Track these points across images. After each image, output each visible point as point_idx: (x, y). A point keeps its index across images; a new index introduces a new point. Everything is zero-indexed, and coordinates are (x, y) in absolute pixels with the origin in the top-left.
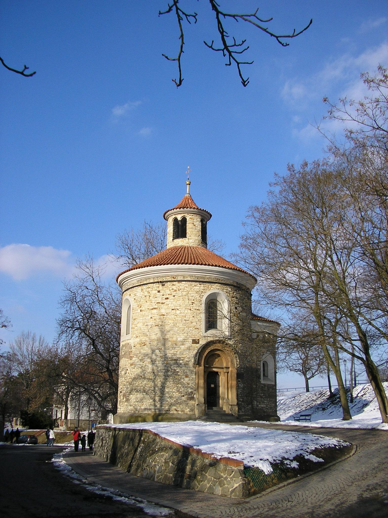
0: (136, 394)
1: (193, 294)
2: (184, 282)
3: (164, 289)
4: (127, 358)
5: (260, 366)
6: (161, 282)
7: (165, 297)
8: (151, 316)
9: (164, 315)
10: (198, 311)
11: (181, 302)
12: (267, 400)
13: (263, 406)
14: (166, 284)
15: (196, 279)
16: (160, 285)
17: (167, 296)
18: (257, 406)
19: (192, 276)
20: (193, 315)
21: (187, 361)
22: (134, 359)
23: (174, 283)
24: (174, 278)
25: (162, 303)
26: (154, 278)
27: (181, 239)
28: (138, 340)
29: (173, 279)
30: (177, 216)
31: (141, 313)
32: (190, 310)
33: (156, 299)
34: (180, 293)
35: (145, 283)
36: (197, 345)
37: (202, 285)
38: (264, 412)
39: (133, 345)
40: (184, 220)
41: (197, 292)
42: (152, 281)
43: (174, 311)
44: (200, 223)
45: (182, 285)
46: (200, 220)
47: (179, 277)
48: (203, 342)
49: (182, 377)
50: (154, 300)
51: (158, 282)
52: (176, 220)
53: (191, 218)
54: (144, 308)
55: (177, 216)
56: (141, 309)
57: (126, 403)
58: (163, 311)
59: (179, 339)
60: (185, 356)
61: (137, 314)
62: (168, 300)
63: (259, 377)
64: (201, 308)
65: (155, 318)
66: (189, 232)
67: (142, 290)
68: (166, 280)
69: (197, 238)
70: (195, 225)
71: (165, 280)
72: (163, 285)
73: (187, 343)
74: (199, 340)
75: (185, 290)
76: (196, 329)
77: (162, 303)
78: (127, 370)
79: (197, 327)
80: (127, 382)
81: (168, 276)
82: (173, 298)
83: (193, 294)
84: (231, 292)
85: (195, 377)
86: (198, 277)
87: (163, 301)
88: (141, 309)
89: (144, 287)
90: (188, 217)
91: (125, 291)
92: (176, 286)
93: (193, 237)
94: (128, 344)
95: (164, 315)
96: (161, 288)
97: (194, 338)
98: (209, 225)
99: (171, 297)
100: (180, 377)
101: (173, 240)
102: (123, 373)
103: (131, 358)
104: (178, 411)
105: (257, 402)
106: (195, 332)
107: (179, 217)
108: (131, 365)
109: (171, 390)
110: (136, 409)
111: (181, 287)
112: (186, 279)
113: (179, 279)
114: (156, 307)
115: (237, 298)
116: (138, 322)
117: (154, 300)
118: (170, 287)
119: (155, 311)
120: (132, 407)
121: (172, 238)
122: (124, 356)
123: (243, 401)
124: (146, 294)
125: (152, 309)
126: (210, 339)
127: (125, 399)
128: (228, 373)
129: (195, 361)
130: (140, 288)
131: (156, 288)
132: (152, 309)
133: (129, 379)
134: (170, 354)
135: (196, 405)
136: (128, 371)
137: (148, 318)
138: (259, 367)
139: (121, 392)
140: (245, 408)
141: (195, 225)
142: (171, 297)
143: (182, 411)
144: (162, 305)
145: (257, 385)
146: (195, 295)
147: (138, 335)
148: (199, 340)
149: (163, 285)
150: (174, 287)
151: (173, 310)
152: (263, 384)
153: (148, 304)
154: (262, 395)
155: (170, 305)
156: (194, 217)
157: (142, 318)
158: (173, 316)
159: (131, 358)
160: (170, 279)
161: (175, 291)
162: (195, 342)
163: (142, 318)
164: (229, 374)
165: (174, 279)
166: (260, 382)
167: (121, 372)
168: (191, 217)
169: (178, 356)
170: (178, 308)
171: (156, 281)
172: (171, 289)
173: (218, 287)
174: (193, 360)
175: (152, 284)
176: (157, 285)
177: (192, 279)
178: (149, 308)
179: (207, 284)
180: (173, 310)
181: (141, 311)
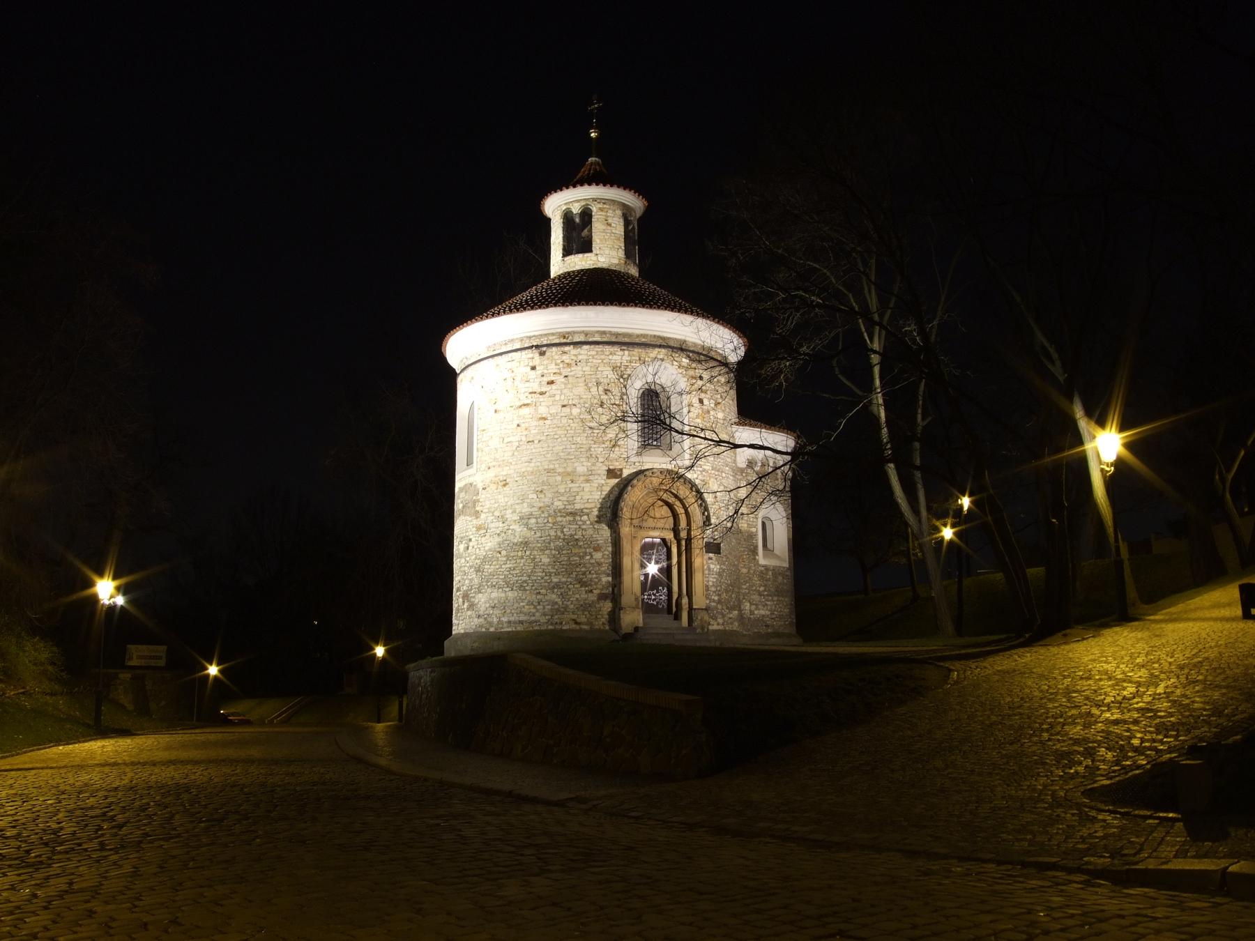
0: (489, 590)
6: (537, 347)
7: (546, 379)
9: (545, 419)
11: (581, 390)
13: (763, 612)
16: (537, 355)
17: (552, 378)
18: (752, 612)
22: (483, 516)
23: (566, 348)
25: (542, 393)
27: (580, 256)
34: (577, 370)
38: (767, 626)
39: (480, 486)
40: (586, 215)
41: (614, 368)
43: (567, 410)
44: (622, 221)
53: (601, 209)
56: (496, 407)
57: (469, 613)
58: (543, 410)
62: (553, 386)
63: (754, 551)
69: (614, 253)
72: (542, 354)
77: (542, 393)
80: (471, 567)
86: (617, 335)
87: (543, 390)
96: (537, 359)
99: (560, 379)
102: (462, 547)
103: (477, 514)
105: (751, 604)
107: (576, 209)
108: (479, 528)
110: (491, 624)
113: (577, 339)
119: (526, 411)
120: (481, 620)
122: (462, 512)
123: (719, 602)
138: (754, 530)
139: (458, 590)
140: (724, 616)
141: (609, 225)
144: (541, 398)
145: (749, 569)
150: (565, 357)
155: (557, 398)
159: (477, 514)
161: (569, 365)
167: (458, 547)
169: (578, 506)
175: (519, 353)
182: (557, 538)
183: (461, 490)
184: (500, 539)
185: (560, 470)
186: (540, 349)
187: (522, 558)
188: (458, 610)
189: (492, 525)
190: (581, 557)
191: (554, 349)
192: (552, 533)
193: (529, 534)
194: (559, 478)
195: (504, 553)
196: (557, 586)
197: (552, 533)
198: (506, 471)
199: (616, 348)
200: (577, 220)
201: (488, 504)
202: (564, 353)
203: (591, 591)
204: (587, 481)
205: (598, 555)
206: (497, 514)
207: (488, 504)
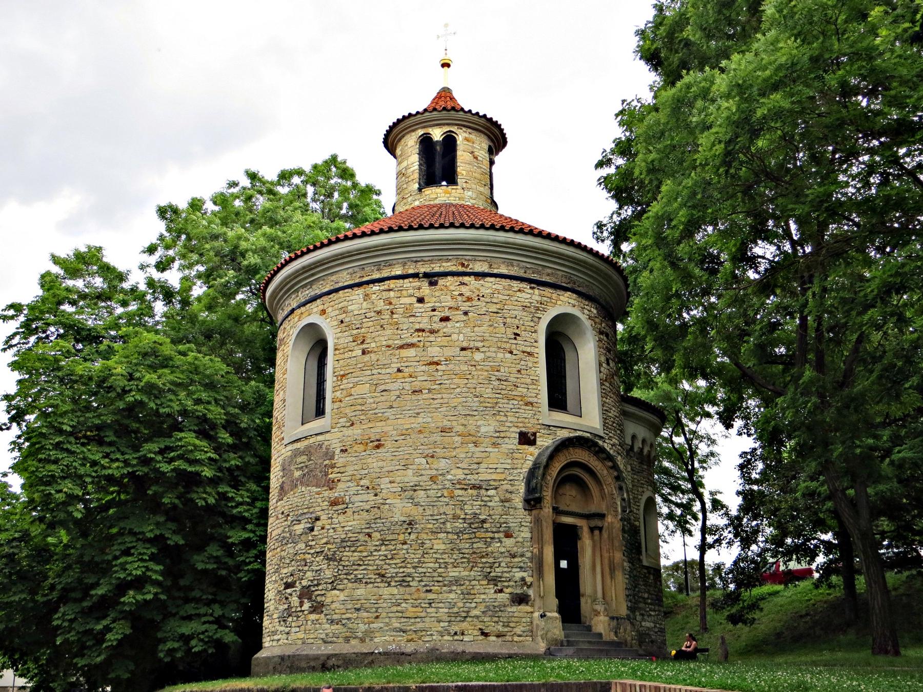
0: (350, 585)
1: (516, 312)
2: (492, 279)
3: (437, 294)
4: (317, 486)
5: (638, 519)
6: (426, 275)
8: (399, 365)
10: (531, 358)
12: (655, 611)
14: (441, 282)
15: (521, 274)
16: (425, 284)
17: (447, 313)
19: (513, 266)
20: (519, 367)
21: (507, 491)
22: (341, 486)
23: (466, 279)
24: (463, 265)
25: (432, 332)
26: (404, 264)
28: (356, 431)
29: (461, 269)
30: (430, 130)
31: (366, 358)
32: (511, 352)
33: (412, 319)
34: (482, 306)
35: (376, 276)
36: (531, 449)
37: (536, 291)
38: (652, 642)
40: (450, 142)
42: (399, 273)
43: (468, 353)
44: (487, 155)
45: (487, 285)
46: (486, 147)
47: (479, 263)
48: (545, 442)
49: (496, 535)
50: (405, 323)
51: (415, 276)
52: (426, 142)
53: (466, 139)
54: (373, 345)
55: (430, 130)
56: (364, 346)
57: (313, 617)
58: (434, 352)
59: (483, 429)
60: (502, 477)
61: (353, 361)
62: (449, 324)
64: (536, 350)
65: (411, 369)
66: (464, 173)
67: (367, 296)
68: (442, 270)
69: (482, 189)
70: (476, 158)
71: (437, 270)
72: (433, 284)
73: (506, 440)
74: (534, 434)
75: (495, 300)
76: (526, 404)
77: (432, 332)
78: (317, 519)
79: (531, 400)
81: (448, 260)
82: (465, 318)
83: (516, 312)
84: (597, 320)
85: (528, 535)
87: (435, 326)
88: (364, 346)
89: (376, 288)
90: (461, 136)
91: (304, 304)
92: (471, 287)
93: (474, 186)
94: (320, 446)
95: (438, 364)
96: (425, 289)
97: (523, 429)
98: (495, 169)
99: (458, 316)
100: (491, 535)
101: (420, 190)
103: (331, 485)
104: (485, 634)
106: (527, 412)
107: (437, 134)
108: (334, 503)
109: (467, 573)
111: (484, 291)
112: (495, 271)
113: (479, 267)
114: (415, 340)
115: (607, 335)
116: (356, 385)
117: (405, 323)
118: (452, 288)
119: (411, 352)
121: (417, 186)
124: (380, 306)
125: (402, 347)
126: (564, 434)
127: (307, 605)
128: (600, 529)
129: (530, 490)
130: (360, 291)
131: (411, 291)
132: (402, 347)
133: (326, 543)
134: (460, 471)
135: (536, 614)
136: (319, 523)
137: (388, 371)
138: (637, 523)
139: (288, 586)
141: (476, 158)
142: (458, 316)
143: (498, 636)
146: (519, 313)
147: (353, 419)
148: (534, 434)
149: (433, 284)
150: (464, 289)
151: (463, 349)
152: (647, 568)
153: (388, 332)
154: (646, 595)
155: (454, 337)
156: (474, 136)
157: (369, 372)
158: (464, 368)
159: (331, 485)
160: (454, 269)
161: (469, 299)
162: (526, 439)
163: (369, 372)
164: (605, 535)
165: (464, 269)
166: (640, 561)
168: (467, 135)
169: (483, 477)
170: (480, 344)
171: (411, 271)
172: (457, 293)
173: (572, 302)
174: (522, 489)
175: (401, 281)
176: (416, 283)
177: (512, 273)
178: (390, 342)
179: (548, 291)
180: (463, 349)
181: (364, 353)
182: (456, 517)
183: (297, 453)
184: (371, 516)
185: (460, 429)
186: (432, 278)
187: (405, 543)
188: (289, 612)
189: (359, 498)
190: (488, 544)
191: (449, 278)
192: (449, 510)
193: (416, 512)
194: (457, 439)
195: (376, 535)
196: (457, 582)
197: (449, 510)
198: (378, 429)
199: (524, 285)
200: (438, 148)
201: (350, 470)
202: (462, 284)
203: (501, 591)
204: (495, 445)
205: (509, 542)
206: (362, 483)
207: (350, 470)
